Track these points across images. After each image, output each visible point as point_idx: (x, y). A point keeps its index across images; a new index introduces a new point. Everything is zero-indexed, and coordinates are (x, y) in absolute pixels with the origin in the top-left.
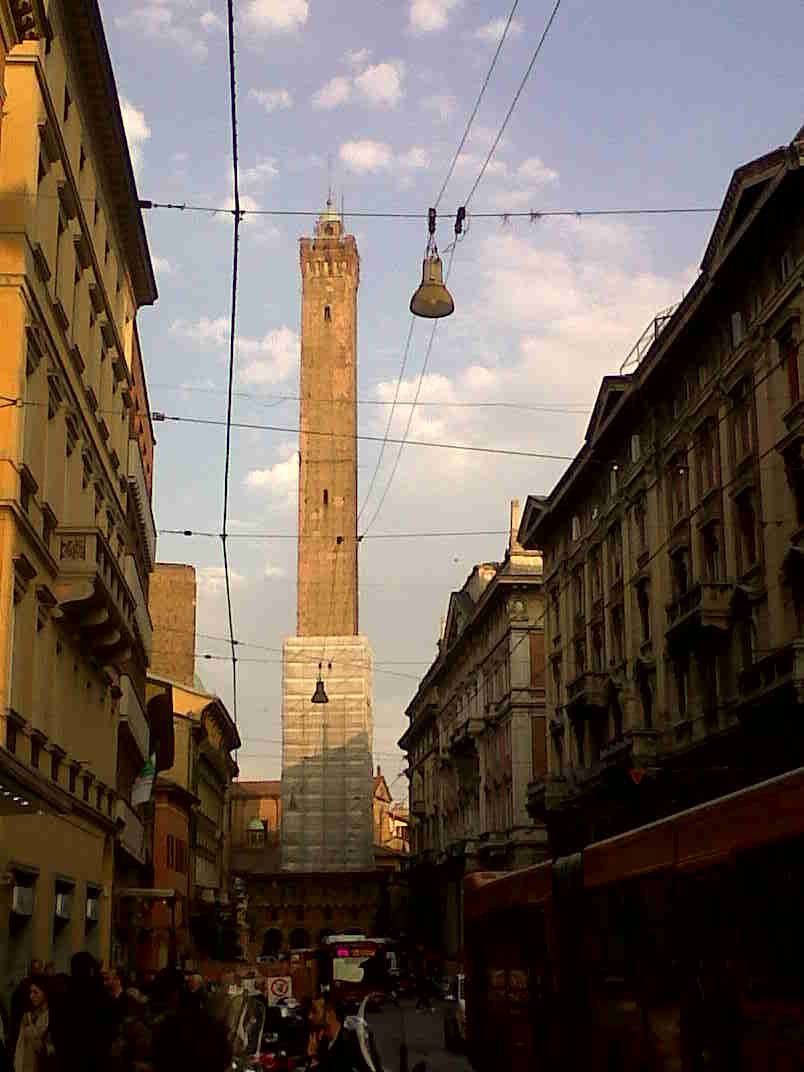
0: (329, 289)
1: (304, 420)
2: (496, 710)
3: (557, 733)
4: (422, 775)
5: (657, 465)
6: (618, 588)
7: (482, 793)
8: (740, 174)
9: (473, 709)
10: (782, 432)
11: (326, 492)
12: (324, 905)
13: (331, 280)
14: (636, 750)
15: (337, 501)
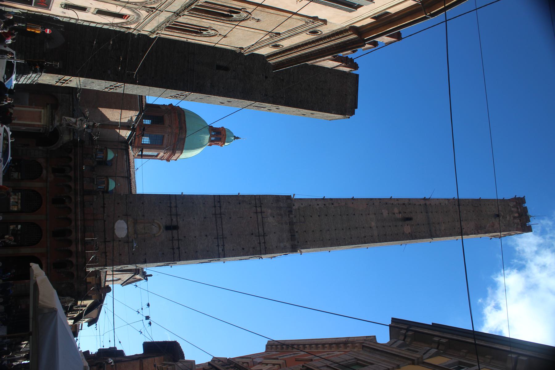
1: (447, 202)
13: (512, 218)
15: (407, 229)
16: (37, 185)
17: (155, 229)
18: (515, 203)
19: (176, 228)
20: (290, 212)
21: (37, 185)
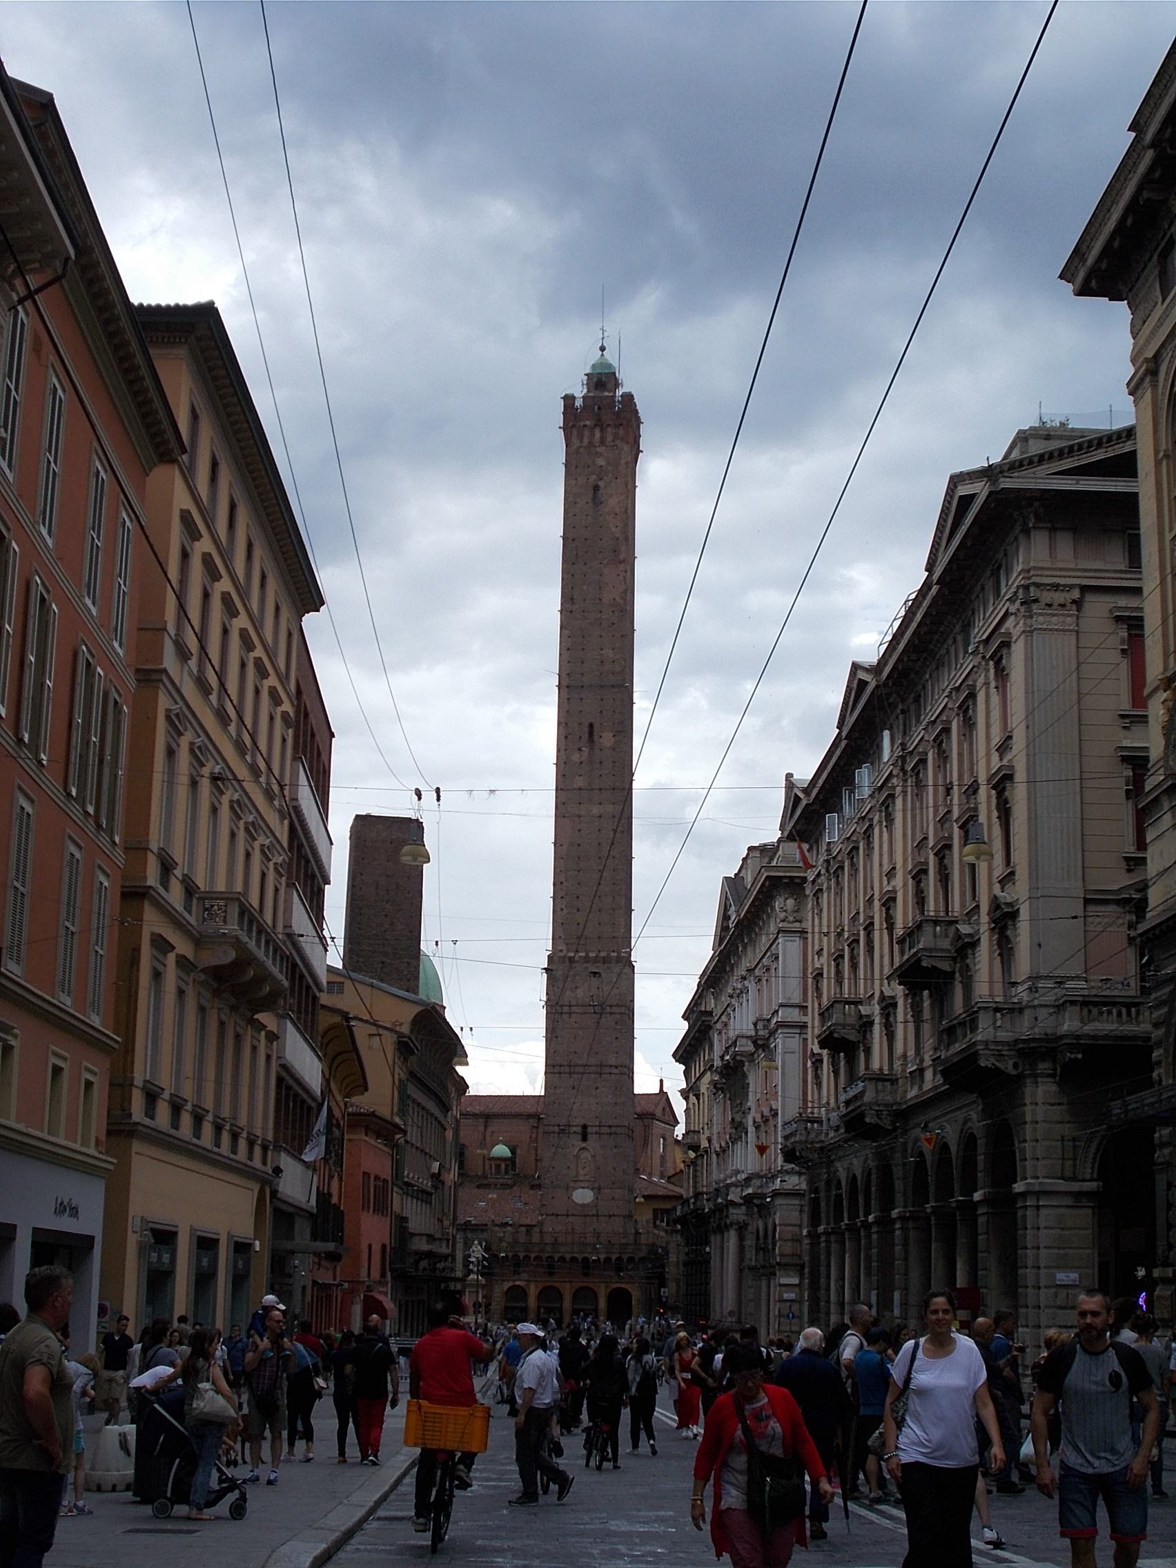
0: (601, 462)
1: (566, 632)
2: (765, 1027)
3: (818, 1062)
4: (698, 1100)
5: (903, 769)
6: (870, 901)
7: (751, 1129)
8: (956, 480)
9: (742, 1021)
10: (996, 763)
11: (591, 726)
12: (580, 1257)
14: (868, 1097)
15: (607, 739)
16: (533, 1292)
17: (585, 1154)
18: (575, 432)
19: (585, 1127)
20: (571, 960)
21: (533, 1292)
